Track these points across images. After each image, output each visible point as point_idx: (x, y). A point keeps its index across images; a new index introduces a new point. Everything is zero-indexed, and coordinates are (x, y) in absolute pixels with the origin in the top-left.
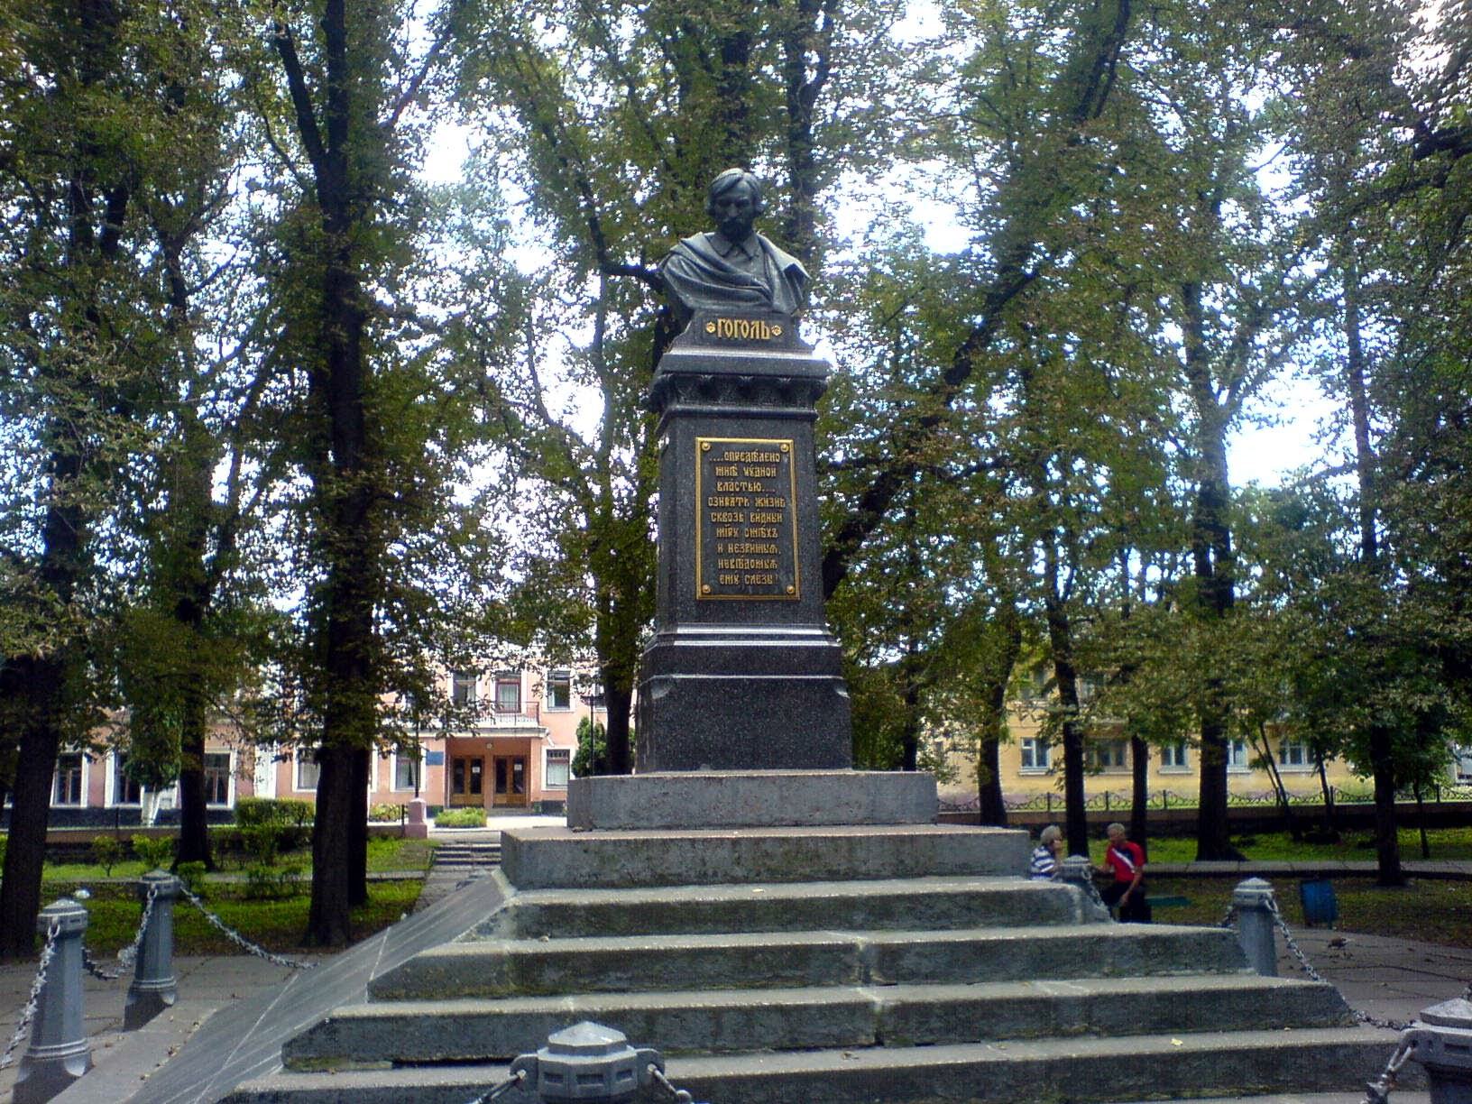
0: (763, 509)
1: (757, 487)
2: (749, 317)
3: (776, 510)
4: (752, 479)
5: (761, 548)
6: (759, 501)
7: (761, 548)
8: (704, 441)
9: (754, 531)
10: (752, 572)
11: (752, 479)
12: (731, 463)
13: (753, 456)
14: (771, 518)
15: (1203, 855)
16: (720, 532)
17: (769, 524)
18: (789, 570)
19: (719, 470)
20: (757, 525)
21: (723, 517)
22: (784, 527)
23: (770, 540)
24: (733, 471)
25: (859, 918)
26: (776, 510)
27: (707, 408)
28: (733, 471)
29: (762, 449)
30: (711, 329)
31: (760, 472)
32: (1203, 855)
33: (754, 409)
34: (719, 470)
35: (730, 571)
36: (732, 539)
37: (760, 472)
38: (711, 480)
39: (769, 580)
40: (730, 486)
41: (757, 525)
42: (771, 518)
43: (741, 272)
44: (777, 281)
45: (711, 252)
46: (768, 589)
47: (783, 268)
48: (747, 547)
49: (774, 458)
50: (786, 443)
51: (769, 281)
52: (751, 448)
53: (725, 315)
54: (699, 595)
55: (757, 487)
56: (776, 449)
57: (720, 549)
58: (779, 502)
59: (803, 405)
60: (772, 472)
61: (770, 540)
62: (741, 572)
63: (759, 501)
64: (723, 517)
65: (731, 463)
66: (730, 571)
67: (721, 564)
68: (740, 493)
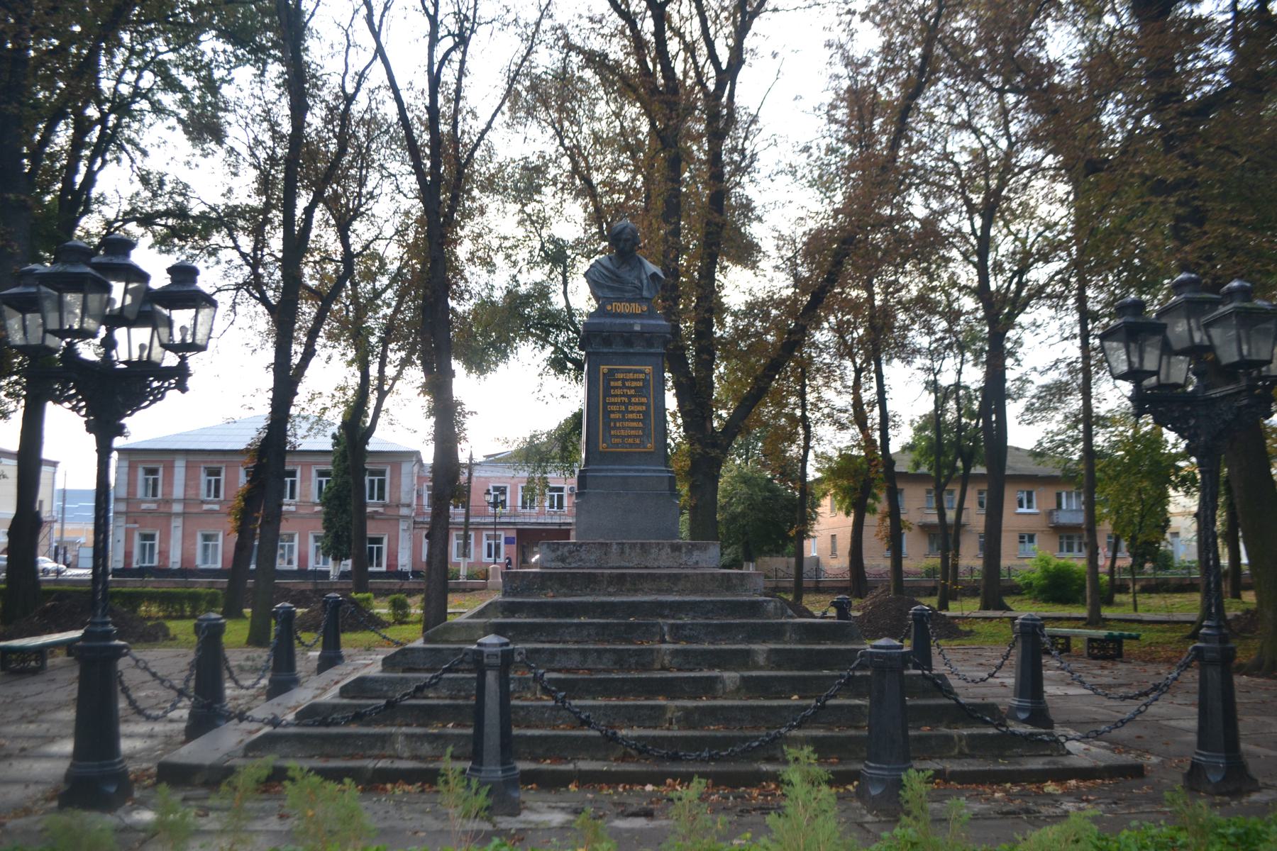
0: (636, 404)
1: (632, 392)
2: (630, 301)
3: (642, 404)
4: (630, 388)
8: (604, 369)
9: (631, 416)
10: (629, 436)
11: (630, 388)
12: (618, 380)
13: (631, 376)
15: (985, 607)
16: (612, 416)
18: (648, 436)
19: (612, 384)
20: (632, 412)
21: (614, 408)
23: (638, 420)
24: (620, 384)
25: (666, 612)
26: (642, 404)
27: (605, 350)
28: (620, 384)
30: (609, 308)
31: (634, 384)
32: (985, 607)
34: (612, 384)
35: (617, 437)
36: (619, 420)
37: (634, 384)
38: (608, 388)
39: (638, 441)
40: (619, 392)
41: (632, 412)
45: (610, 266)
46: (638, 446)
48: (626, 424)
49: (642, 376)
50: (648, 369)
51: (641, 282)
52: (629, 371)
53: (619, 300)
55: (632, 392)
58: (644, 400)
60: (641, 384)
61: (638, 420)
62: (623, 437)
64: (614, 408)
65: (618, 380)
66: (617, 437)
68: (623, 395)
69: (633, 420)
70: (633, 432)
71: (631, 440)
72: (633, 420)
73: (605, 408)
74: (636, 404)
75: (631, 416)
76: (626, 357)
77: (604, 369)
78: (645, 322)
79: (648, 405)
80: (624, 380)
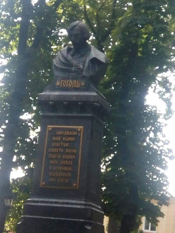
0: (68, 153)
1: (67, 145)
4: (66, 142)
5: (66, 169)
6: (67, 150)
7: (66, 169)
8: (50, 127)
9: (64, 162)
11: (66, 142)
12: (58, 136)
13: (67, 133)
14: (71, 157)
16: (51, 162)
17: (70, 159)
19: (54, 138)
21: (54, 156)
22: (75, 161)
23: (69, 166)
24: (59, 138)
26: (73, 154)
28: (59, 138)
29: (71, 130)
33: (70, 115)
34: (54, 138)
38: (50, 141)
39: (67, 181)
40: (58, 145)
41: (65, 159)
42: (71, 157)
43: (74, 62)
44: (87, 64)
47: (90, 58)
48: (60, 168)
49: (75, 133)
50: (80, 128)
54: (41, 186)
55: (67, 145)
56: (75, 130)
57: (50, 168)
58: (75, 151)
59: (89, 113)
60: (74, 139)
61: (69, 166)
63: (67, 150)
64: (54, 156)
65: (58, 136)
67: (50, 174)
69: (65, 165)
70: (64, 174)
71: (62, 180)
72: (65, 165)
73: (47, 156)
74: (68, 153)
75: (64, 162)
76: (67, 120)
77: (50, 127)
78: (82, 93)
79: (76, 154)
80: (62, 136)
